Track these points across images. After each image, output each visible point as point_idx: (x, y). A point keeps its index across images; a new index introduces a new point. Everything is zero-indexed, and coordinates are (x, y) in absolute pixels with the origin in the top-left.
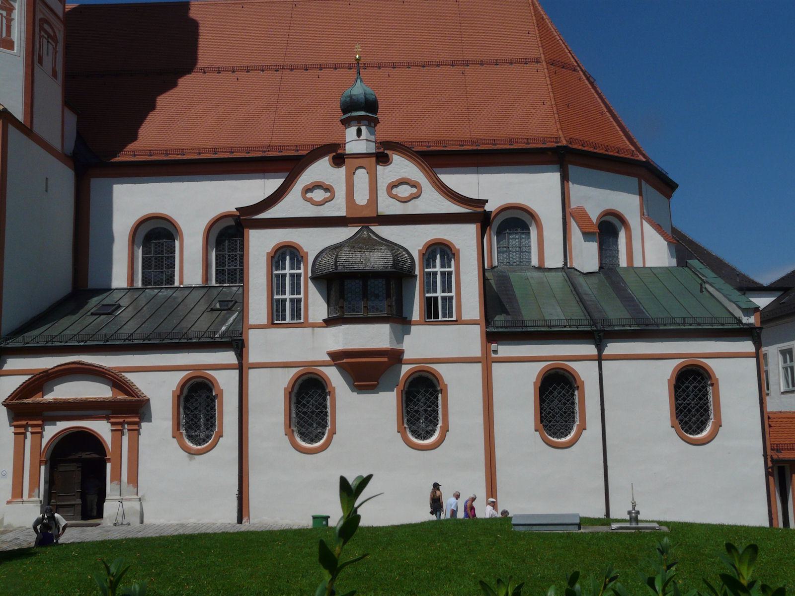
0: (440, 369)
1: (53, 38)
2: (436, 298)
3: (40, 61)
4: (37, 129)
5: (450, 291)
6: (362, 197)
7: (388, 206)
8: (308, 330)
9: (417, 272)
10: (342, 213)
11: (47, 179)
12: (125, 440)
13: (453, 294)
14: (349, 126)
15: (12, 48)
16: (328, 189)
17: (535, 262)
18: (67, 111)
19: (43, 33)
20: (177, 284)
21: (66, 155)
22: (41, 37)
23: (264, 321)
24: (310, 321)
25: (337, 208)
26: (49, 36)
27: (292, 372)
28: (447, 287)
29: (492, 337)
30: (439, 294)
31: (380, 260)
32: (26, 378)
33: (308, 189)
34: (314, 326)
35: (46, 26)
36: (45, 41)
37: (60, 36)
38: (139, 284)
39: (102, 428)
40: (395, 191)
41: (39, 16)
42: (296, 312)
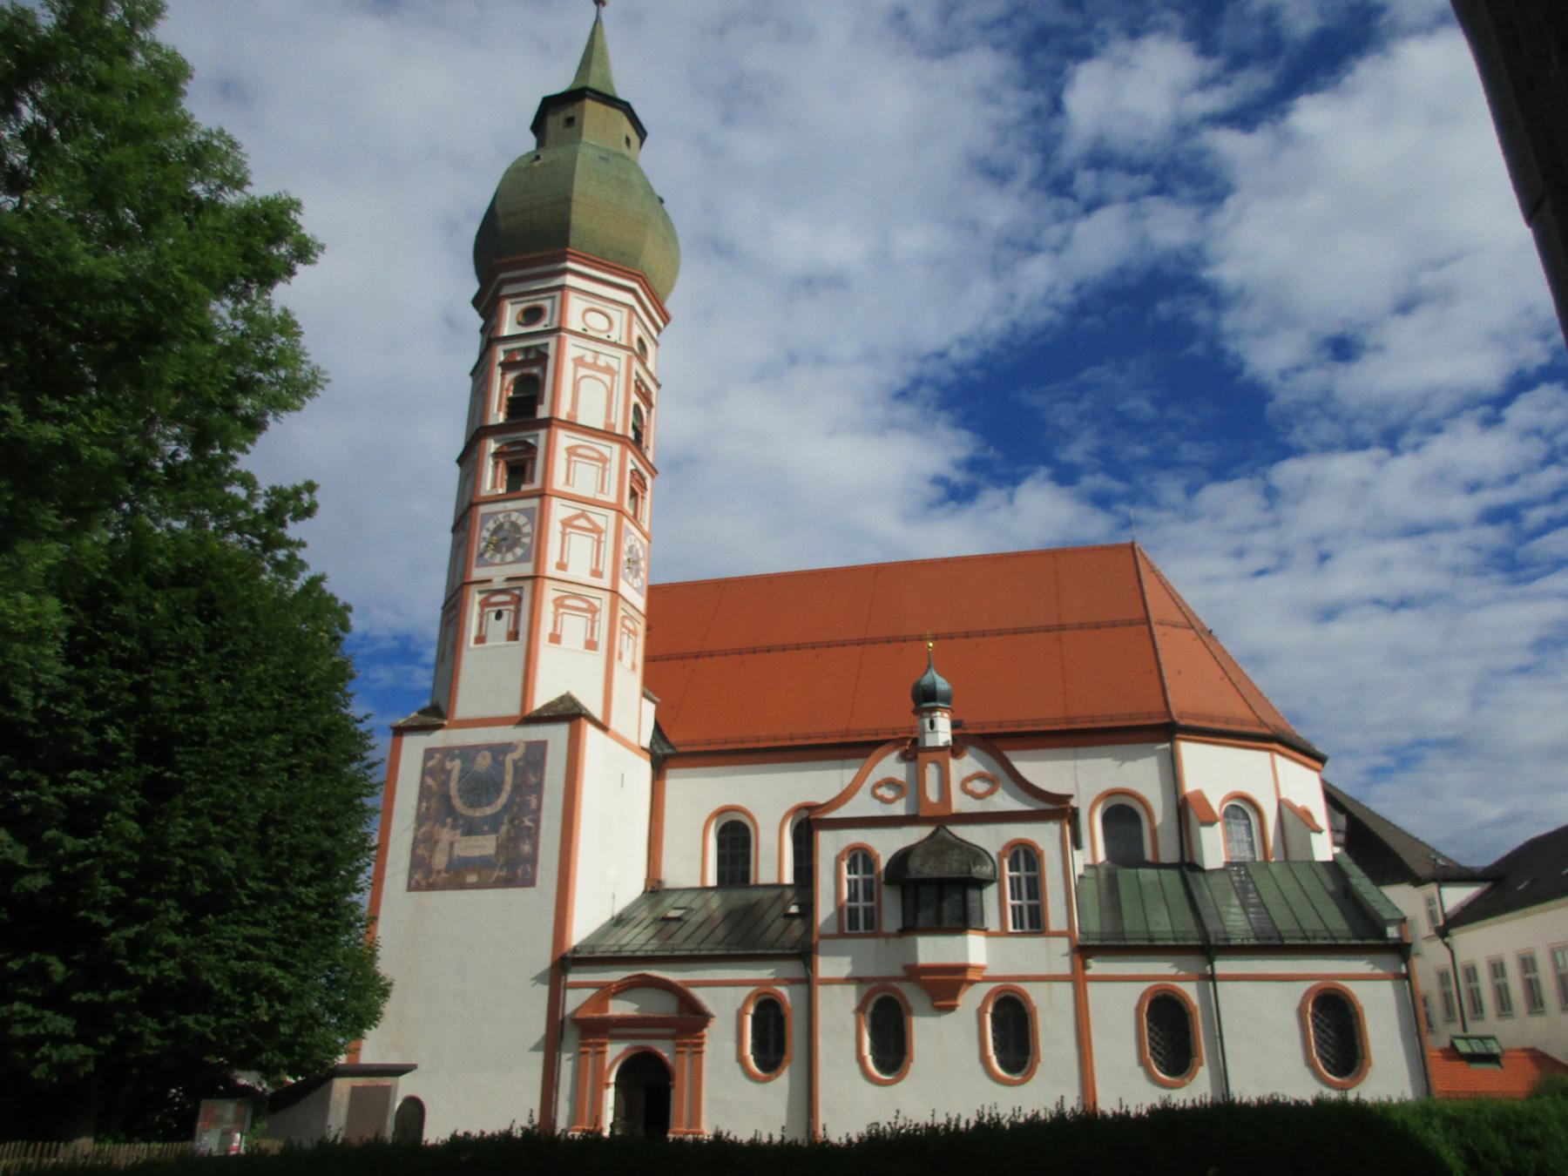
0: (1026, 987)
1: (634, 633)
3: (620, 658)
4: (614, 725)
6: (932, 794)
7: (960, 803)
8: (882, 941)
11: (623, 775)
12: (687, 1061)
14: (922, 717)
17: (1148, 856)
18: (646, 702)
19: (624, 630)
21: (643, 749)
22: (622, 633)
23: (833, 930)
26: (630, 631)
29: (1083, 951)
31: (951, 867)
33: (879, 785)
34: (888, 936)
35: (628, 623)
36: (626, 637)
37: (641, 629)
38: (712, 880)
39: (664, 1049)
40: (970, 786)
41: (621, 613)
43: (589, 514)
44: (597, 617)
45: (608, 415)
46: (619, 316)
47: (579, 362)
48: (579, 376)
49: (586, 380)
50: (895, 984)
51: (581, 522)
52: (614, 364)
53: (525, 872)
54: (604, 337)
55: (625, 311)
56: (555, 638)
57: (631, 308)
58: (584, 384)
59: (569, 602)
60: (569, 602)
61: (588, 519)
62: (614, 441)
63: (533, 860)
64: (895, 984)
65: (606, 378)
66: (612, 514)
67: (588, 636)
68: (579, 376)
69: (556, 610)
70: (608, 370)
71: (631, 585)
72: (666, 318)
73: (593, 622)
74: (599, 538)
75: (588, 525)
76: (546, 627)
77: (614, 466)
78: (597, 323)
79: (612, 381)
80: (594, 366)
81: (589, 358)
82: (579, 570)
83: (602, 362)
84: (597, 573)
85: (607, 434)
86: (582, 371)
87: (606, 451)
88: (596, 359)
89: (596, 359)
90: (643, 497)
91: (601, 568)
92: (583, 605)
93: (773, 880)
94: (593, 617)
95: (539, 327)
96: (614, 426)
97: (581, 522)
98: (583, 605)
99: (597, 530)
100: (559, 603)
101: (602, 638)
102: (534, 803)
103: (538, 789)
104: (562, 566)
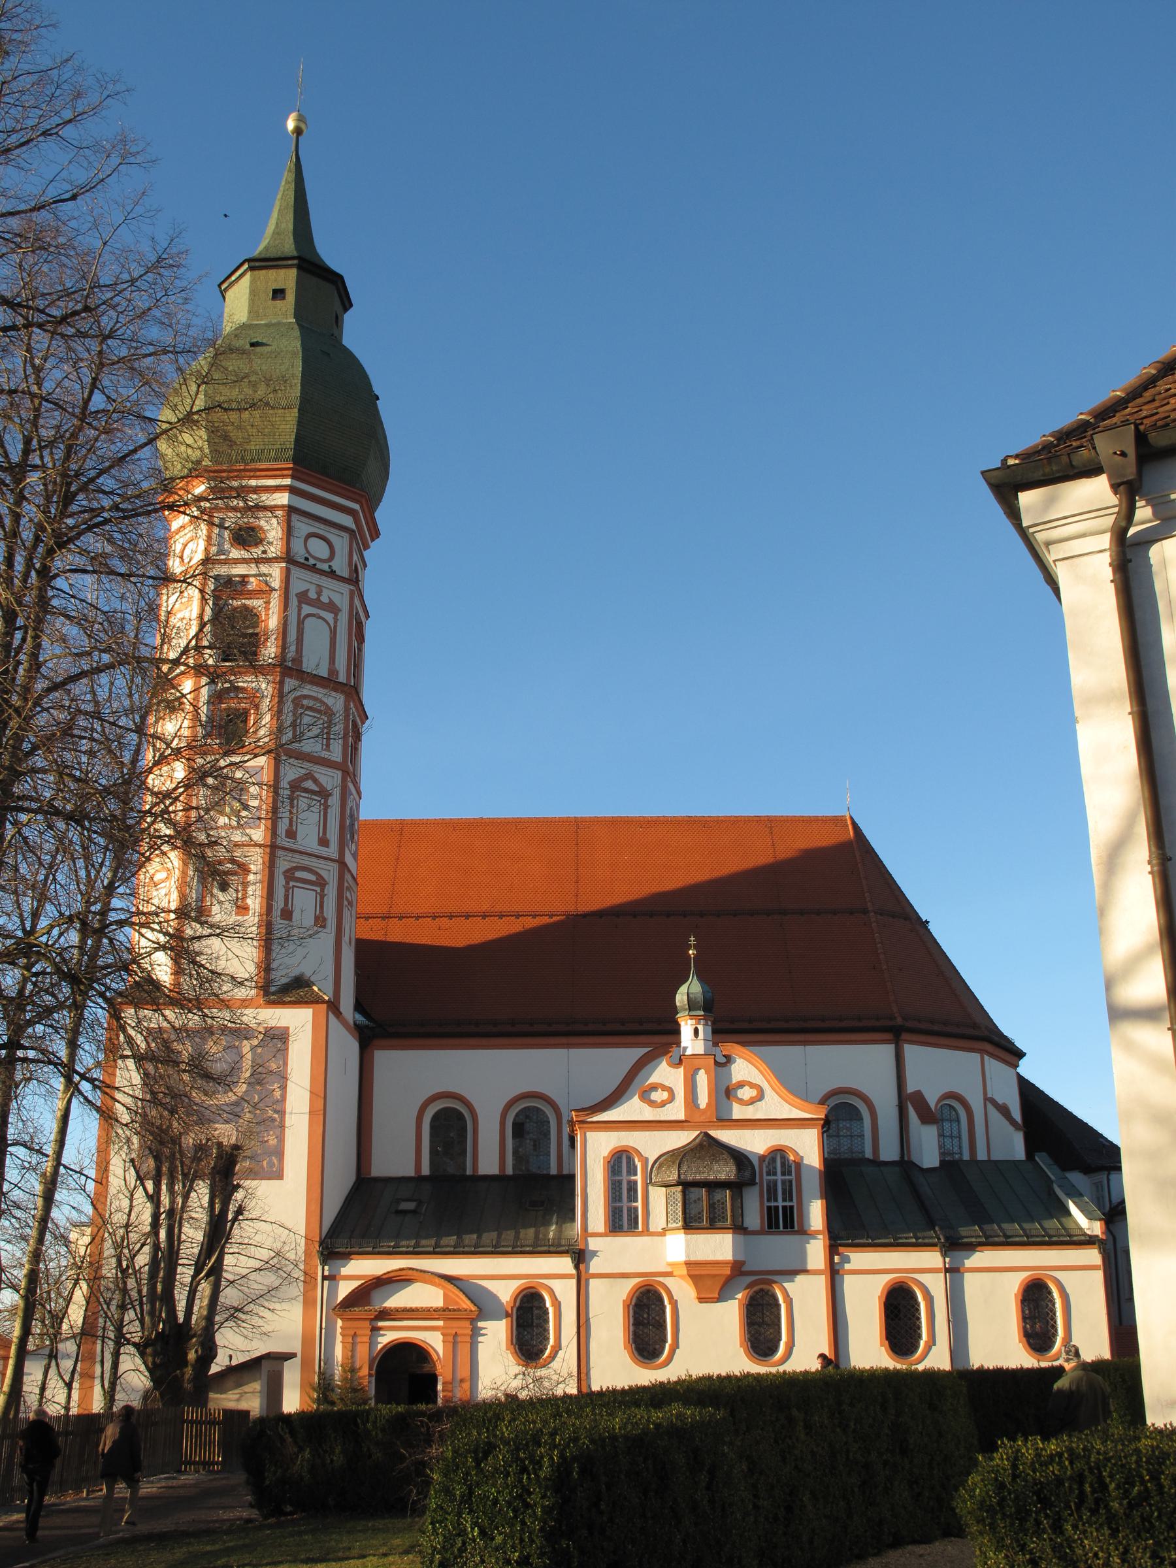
2: (777, 1208)
5: (791, 1200)
6: (703, 1100)
9: (757, 1180)
10: (682, 1117)
13: (794, 1203)
15: (324, 927)
16: (665, 1088)
20: (469, 1172)
24: (652, 1229)
25: (676, 1111)
27: (633, 1282)
28: (788, 1195)
30: (780, 1203)
31: (725, 1171)
32: (356, 1284)
42: (634, 1222)
43: (317, 776)
44: (326, 892)
45: (332, 659)
47: (303, 597)
48: (303, 613)
49: (310, 619)
50: (661, 1279)
51: (309, 784)
52: (337, 599)
53: (271, 1164)
54: (325, 567)
55: (346, 536)
56: (287, 914)
58: (309, 622)
59: (299, 874)
60: (299, 874)
61: (315, 781)
62: (335, 690)
63: (280, 1153)
64: (661, 1279)
65: (329, 617)
66: (338, 775)
68: (303, 613)
69: (287, 883)
70: (332, 607)
72: (375, 533)
73: (322, 896)
76: (279, 904)
77: (339, 718)
78: (319, 549)
79: (336, 622)
80: (317, 603)
81: (312, 595)
82: (308, 838)
83: (324, 599)
84: (324, 842)
85: (329, 682)
86: (307, 609)
87: (330, 701)
88: (319, 593)
89: (319, 593)
91: (328, 835)
92: (313, 878)
93: (495, 1171)
94: (322, 890)
95: (257, 552)
98: (313, 878)
99: (324, 794)
100: (289, 875)
101: (330, 912)
102: (278, 1094)
103: (283, 1078)
104: (291, 834)
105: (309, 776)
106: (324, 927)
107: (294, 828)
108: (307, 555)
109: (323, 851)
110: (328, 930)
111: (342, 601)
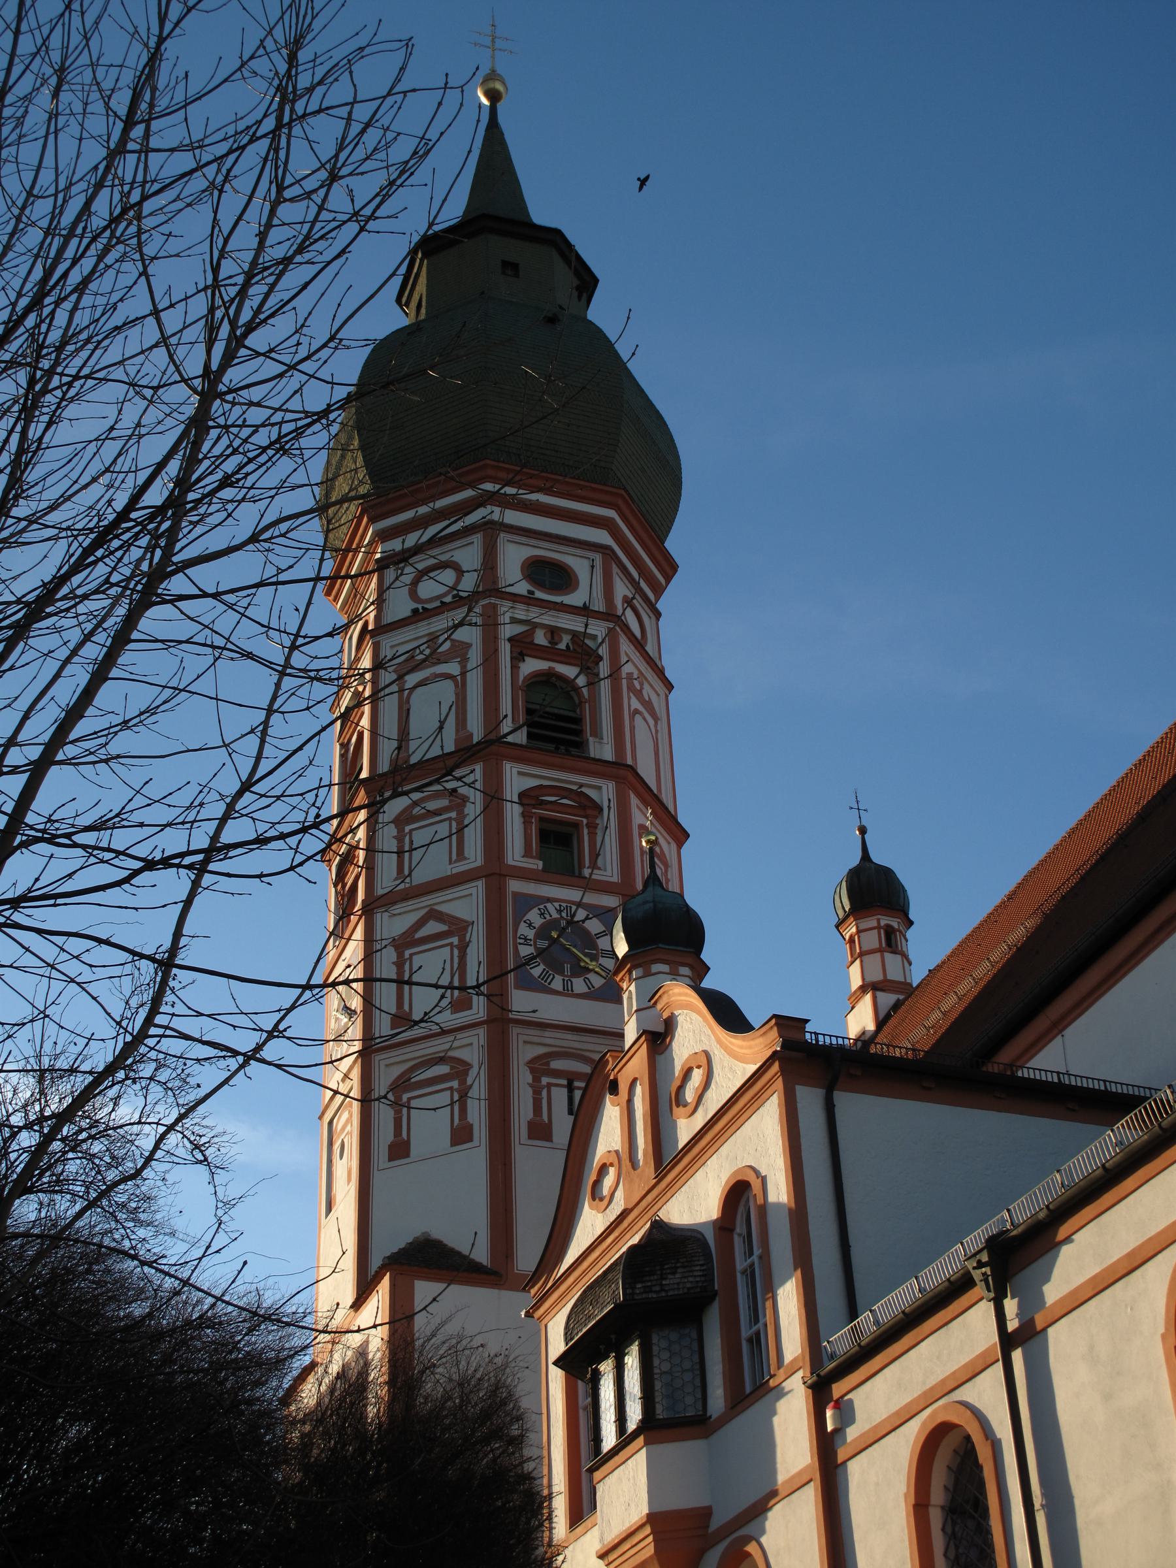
15: (471, 1140)
43: (442, 908)
46: (469, 555)
51: (433, 927)
52: (462, 634)
56: (400, 1150)
57: (490, 529)
65: (453, 668)
67: (456, 1121)
71: (568, 992)
74: (462, 939)
75: (443, 928)
80: (435, 658)
86: (411, 680)
90: (592, 827)
92: (443, 1069)
94: (463, 1082)
96: (471, 735)
97: (433, 927)
98: (443, 1069)
101: (477, 1114)
105: (433, 915)
106: (471, 1140)
107: (406, 1008)
108: (415, 605)
109: (464, 1017)
110: (476, 1142)
111: (470, 635)
